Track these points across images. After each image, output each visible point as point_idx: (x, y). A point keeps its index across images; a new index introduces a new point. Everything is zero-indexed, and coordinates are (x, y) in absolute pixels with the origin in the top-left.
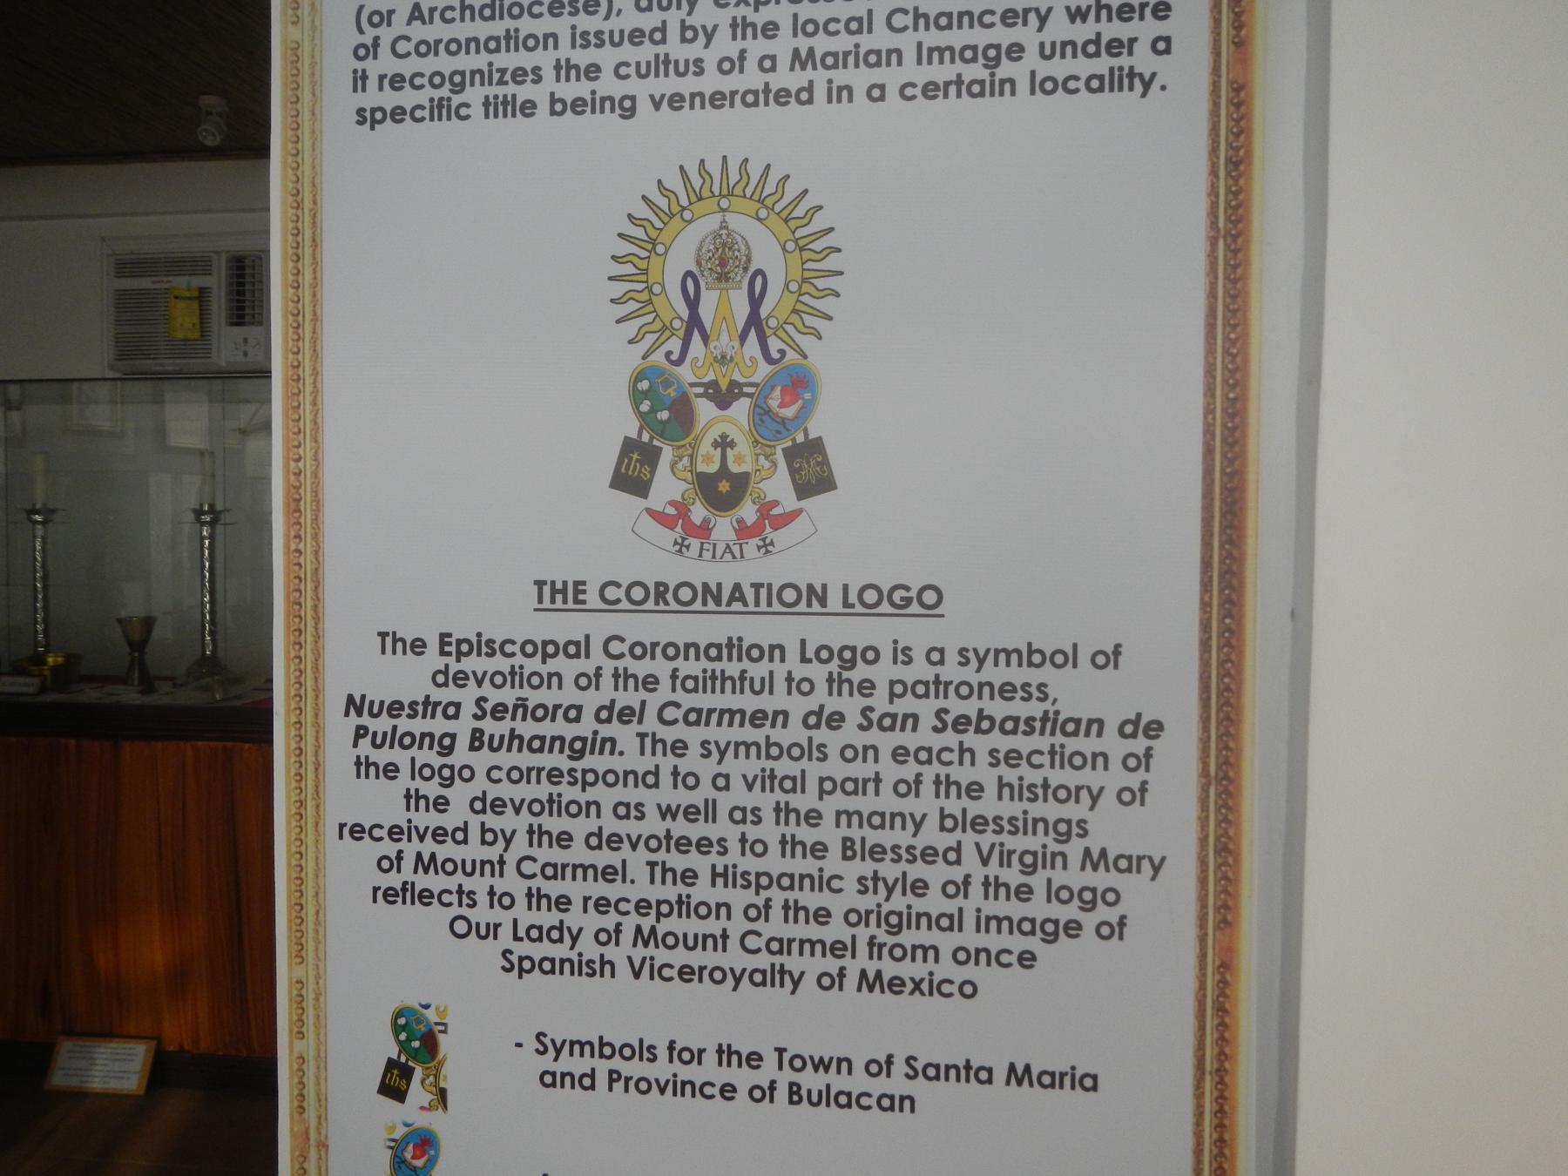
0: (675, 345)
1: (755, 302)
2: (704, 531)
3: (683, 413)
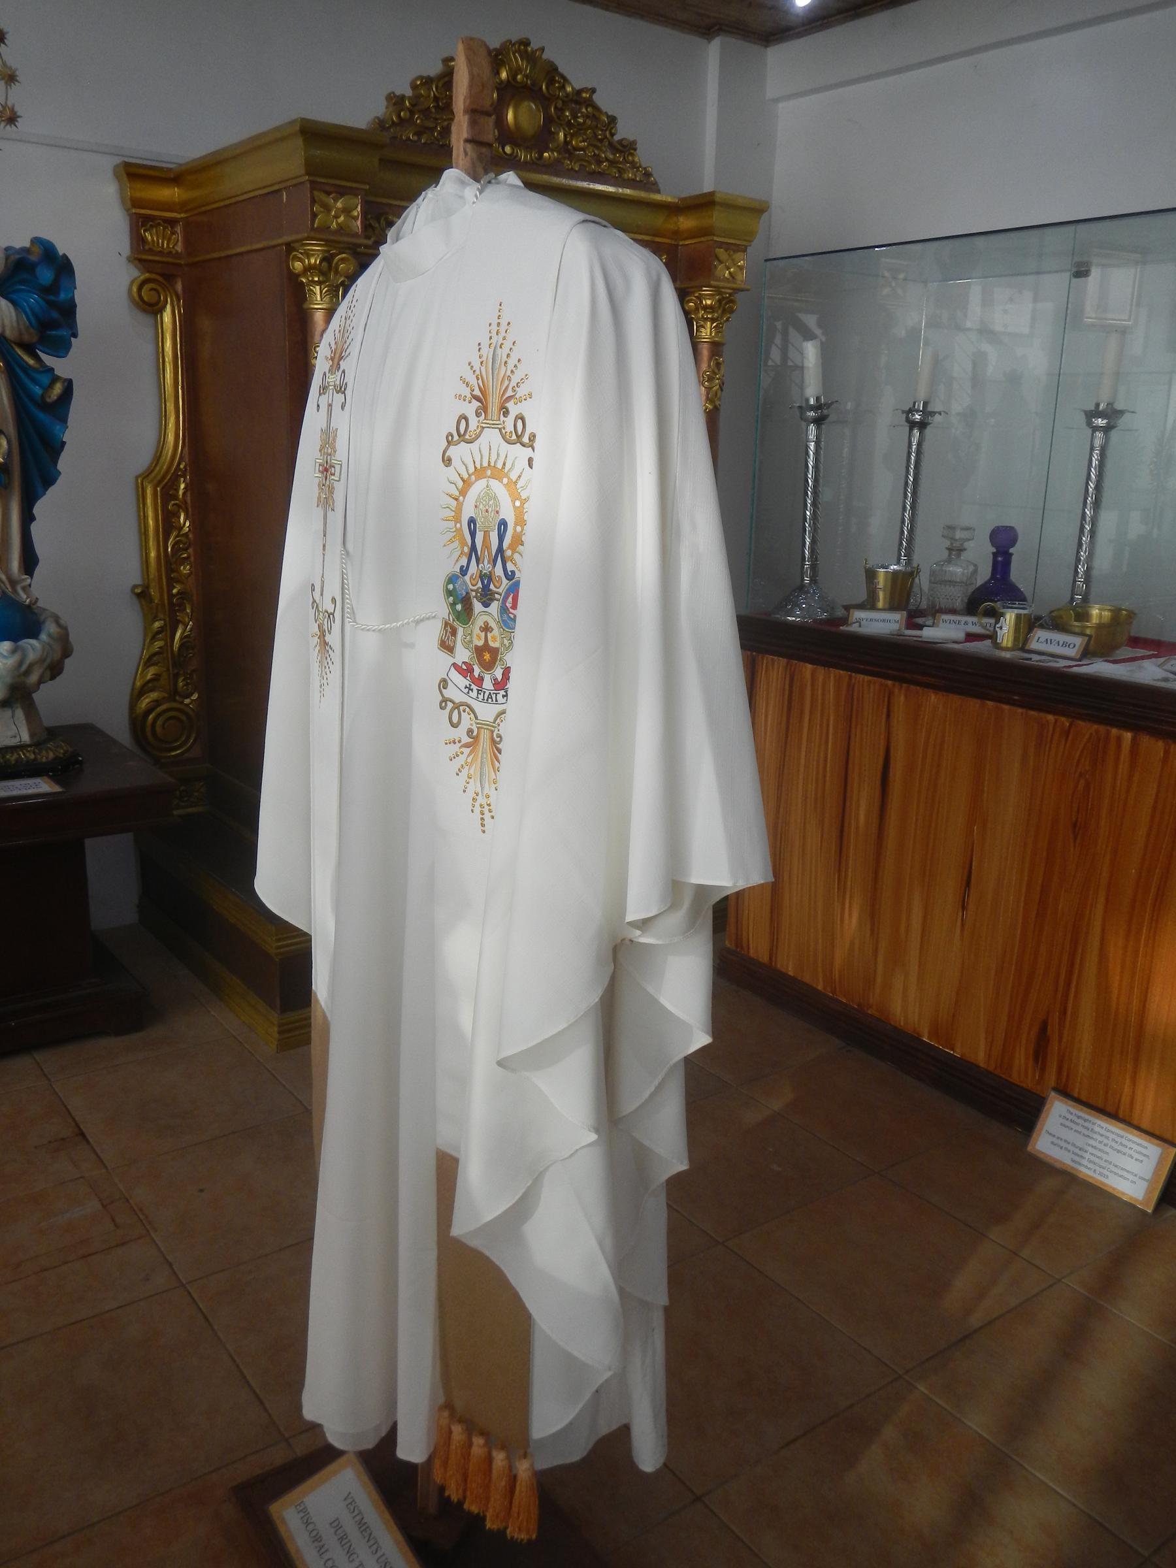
0: (464, 561)
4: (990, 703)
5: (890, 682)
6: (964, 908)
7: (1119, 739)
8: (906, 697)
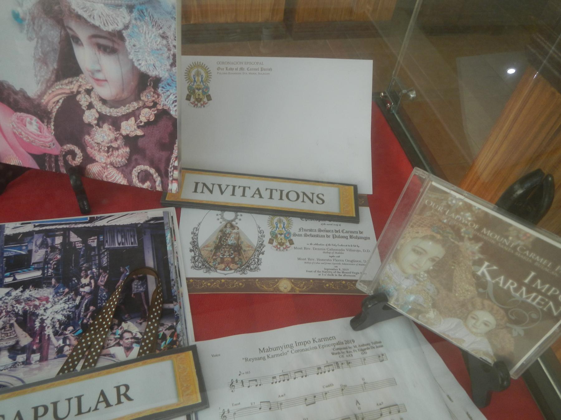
1: (284, 225)
2: (279, 248)
3: (276, 236)
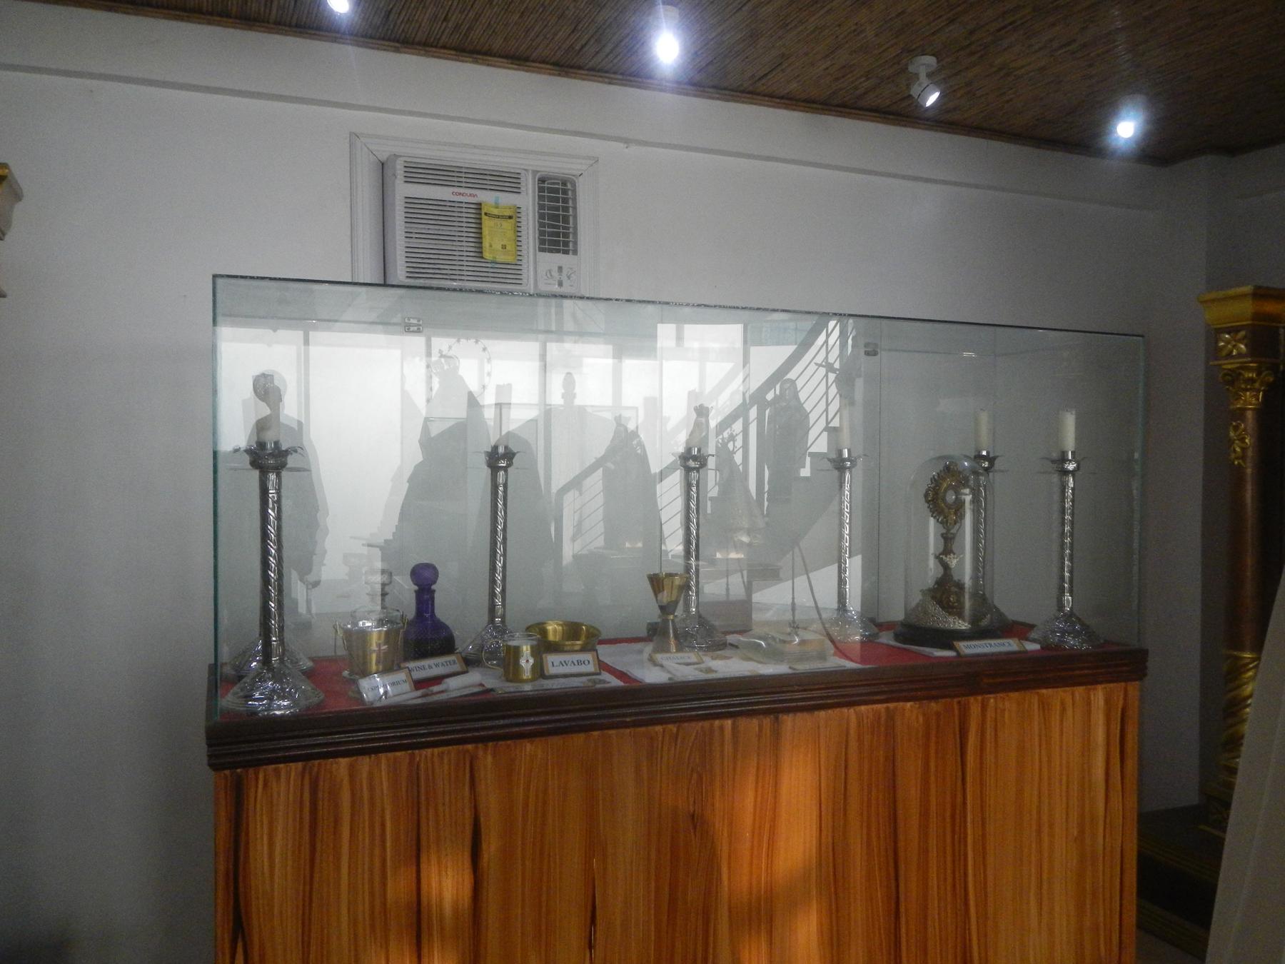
4: (596, 733)
5: (470, 747)
6: (591, 947)
7: (722, 728)
8: (494, 756)
